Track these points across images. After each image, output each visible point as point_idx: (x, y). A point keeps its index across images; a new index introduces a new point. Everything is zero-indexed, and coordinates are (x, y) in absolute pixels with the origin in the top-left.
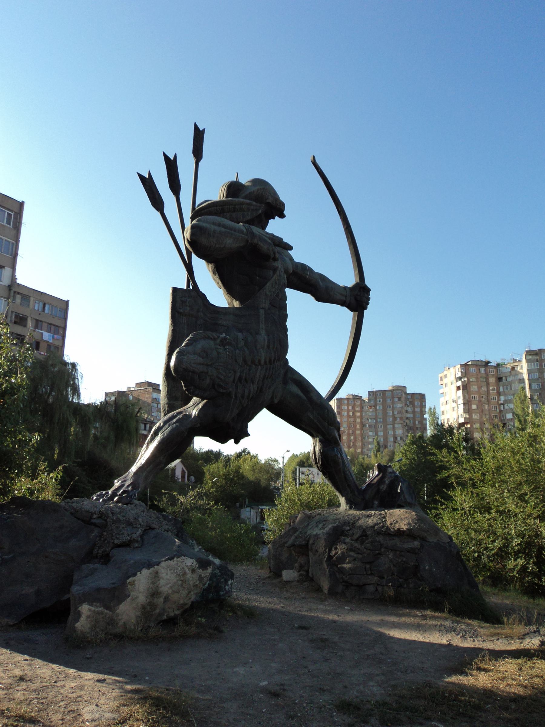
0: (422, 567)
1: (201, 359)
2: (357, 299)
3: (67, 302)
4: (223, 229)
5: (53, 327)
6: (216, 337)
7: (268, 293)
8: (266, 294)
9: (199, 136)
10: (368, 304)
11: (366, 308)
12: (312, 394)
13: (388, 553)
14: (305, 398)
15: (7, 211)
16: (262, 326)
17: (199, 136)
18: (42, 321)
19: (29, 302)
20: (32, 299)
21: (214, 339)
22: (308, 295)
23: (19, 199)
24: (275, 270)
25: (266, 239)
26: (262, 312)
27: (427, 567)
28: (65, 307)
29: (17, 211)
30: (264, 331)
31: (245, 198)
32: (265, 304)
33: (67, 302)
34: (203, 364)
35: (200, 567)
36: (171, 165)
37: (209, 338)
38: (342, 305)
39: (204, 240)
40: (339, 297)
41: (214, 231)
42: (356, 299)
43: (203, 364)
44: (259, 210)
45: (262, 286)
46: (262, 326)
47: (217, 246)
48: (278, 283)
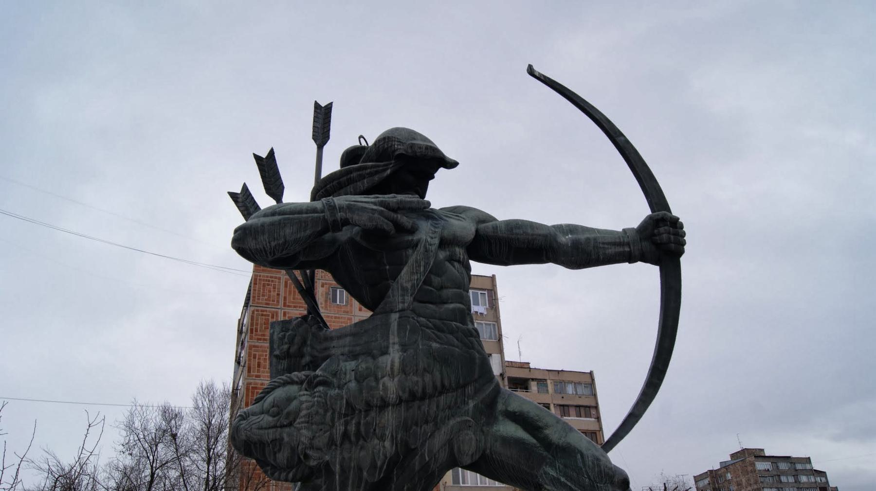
1: (270, 419)
2: (659, 242)
3: (591, 373)
4: (277, 218)
5: (582, 410)
6: (304, 377)
7: (405, 285)
9: (323, 118)
10: (683, 243)
11: (681, 252)
12: (547, 432)
14: (534, 441)
15: (480, 292)
16: (394, 338)
17: (323, 118)
18: (568, 406)
19: (547, 386)
20: (549, 382)
21: (301, 383)
22: (551, 266)
23: (490, 275)
24: (415, 245)
25: (366, 205)
26: (395, 317)
28: (590, 381)
29: (489, 287)
30: (397, 347)
31: (363, 162)
32: (403, 303)
33: (591, 373)
34: (275, 427)
36: (268, 167)
37: (292, 382)
38: (631, 259)
39: (251, 244)
40: (612, 250)
41: (263, 225)
42: (655, 243)
43: (275, 427)
45: (395, 277)
46: (394, 338)
47: (273, 244)
48: (422, 263)
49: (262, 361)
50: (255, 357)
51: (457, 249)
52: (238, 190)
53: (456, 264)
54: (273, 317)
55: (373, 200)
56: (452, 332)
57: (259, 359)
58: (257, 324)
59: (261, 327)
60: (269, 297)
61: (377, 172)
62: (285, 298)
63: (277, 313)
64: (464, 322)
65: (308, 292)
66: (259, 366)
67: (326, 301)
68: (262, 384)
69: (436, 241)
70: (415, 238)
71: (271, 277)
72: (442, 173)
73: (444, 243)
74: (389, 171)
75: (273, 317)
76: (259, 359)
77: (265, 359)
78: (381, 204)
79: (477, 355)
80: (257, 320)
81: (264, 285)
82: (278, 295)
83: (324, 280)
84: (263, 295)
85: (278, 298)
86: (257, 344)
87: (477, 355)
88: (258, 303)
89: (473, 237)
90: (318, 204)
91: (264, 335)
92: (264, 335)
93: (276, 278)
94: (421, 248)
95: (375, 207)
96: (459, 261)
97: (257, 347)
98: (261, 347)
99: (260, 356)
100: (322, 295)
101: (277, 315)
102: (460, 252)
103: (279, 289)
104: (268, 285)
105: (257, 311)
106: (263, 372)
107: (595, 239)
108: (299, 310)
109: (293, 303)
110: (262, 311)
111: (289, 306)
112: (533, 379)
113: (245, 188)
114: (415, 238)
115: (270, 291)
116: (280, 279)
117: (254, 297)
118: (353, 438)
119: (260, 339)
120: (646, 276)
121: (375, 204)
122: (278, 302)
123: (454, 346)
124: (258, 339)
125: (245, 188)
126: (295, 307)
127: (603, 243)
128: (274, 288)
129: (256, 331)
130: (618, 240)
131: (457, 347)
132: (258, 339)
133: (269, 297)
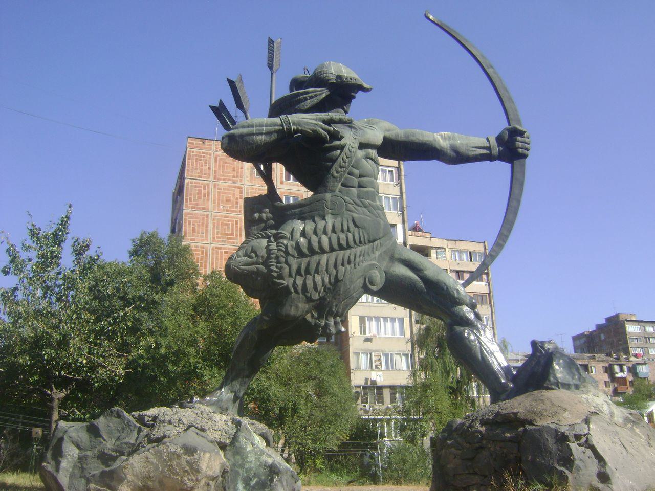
0: (523, 458)
8: (334, 177)
12: (426, 272)
13: (489, 446)
14: (418, 278)
20: (447, 250)
24: (342, 148)
27: (530, 458)
35: (185, 454)
44: (323, 93)
49: (196, 227)
50: (190, 223)
51: (370, 151)
52: (217, 105)
53: (369, 160)
54: (205, 189)
55: (314, 117)
56: (365, 207)
57: (194, 225)
58: (191, 195)
59: (195, 196)
60: (202, 170)
61: (316, 96)
62: (215, 172)
63: (208, 185)
64: (374, 200)
65: (267, 177)
66: (193, 231)
67: (251, 175)
68: (197, 247)
69: (357, 145)
70: (343, 142)
71: (203, 153)
72: (360, 95)
73: (362, 146)
74: (324, 95)
75: (205, 189)
76: (194, 225)
77: (199, 225)
78: (319, 120)
79: (382, 222)
80: (191, 191)
81: (197, 160)
82: (209, 169)
83: (278, 169)
84: (196, 169)
85: (209, 172)
86: (191, 212)
87: (382, 222)
88: (192, 176)
89: (381, 142)
90: (277, 120)
91: (197, 204)
92: (197, 204)
93: (207, 154)
94: (346, 150)
95: (315, 122)
96: (371, 159)
97: (191, 214)
98: (195, 214)
99: (194, 221)
100: (248, 169)
101: (208, 187)
102: (373, 153)
103: (210, 163)
104: (200, 160)
105: (191, 183)
106: (197, 236)
107: (466, 144)
108: (263, 189)
109: (222, 176)
110: (195, 183)
111: (219, 179)
112: (433, 247)
113: (221, 103)
114: (343, 142)
115: (202, 166)
116: (210, 154)
117: (188, 170)
118: (303, 272)
119: (194, 208)
120: (502, 168)
121: (316, 120)
122: (209, 175)
123: (367, 216)
124: (194, 208)
125: (221, 103)
126: (224, 180)
127: (473, 147)
128: (206, 163)
129: (191, 200)
130: (482, 146)
131: (369, 216)
132: (193, 208)
133: (202, 170)
